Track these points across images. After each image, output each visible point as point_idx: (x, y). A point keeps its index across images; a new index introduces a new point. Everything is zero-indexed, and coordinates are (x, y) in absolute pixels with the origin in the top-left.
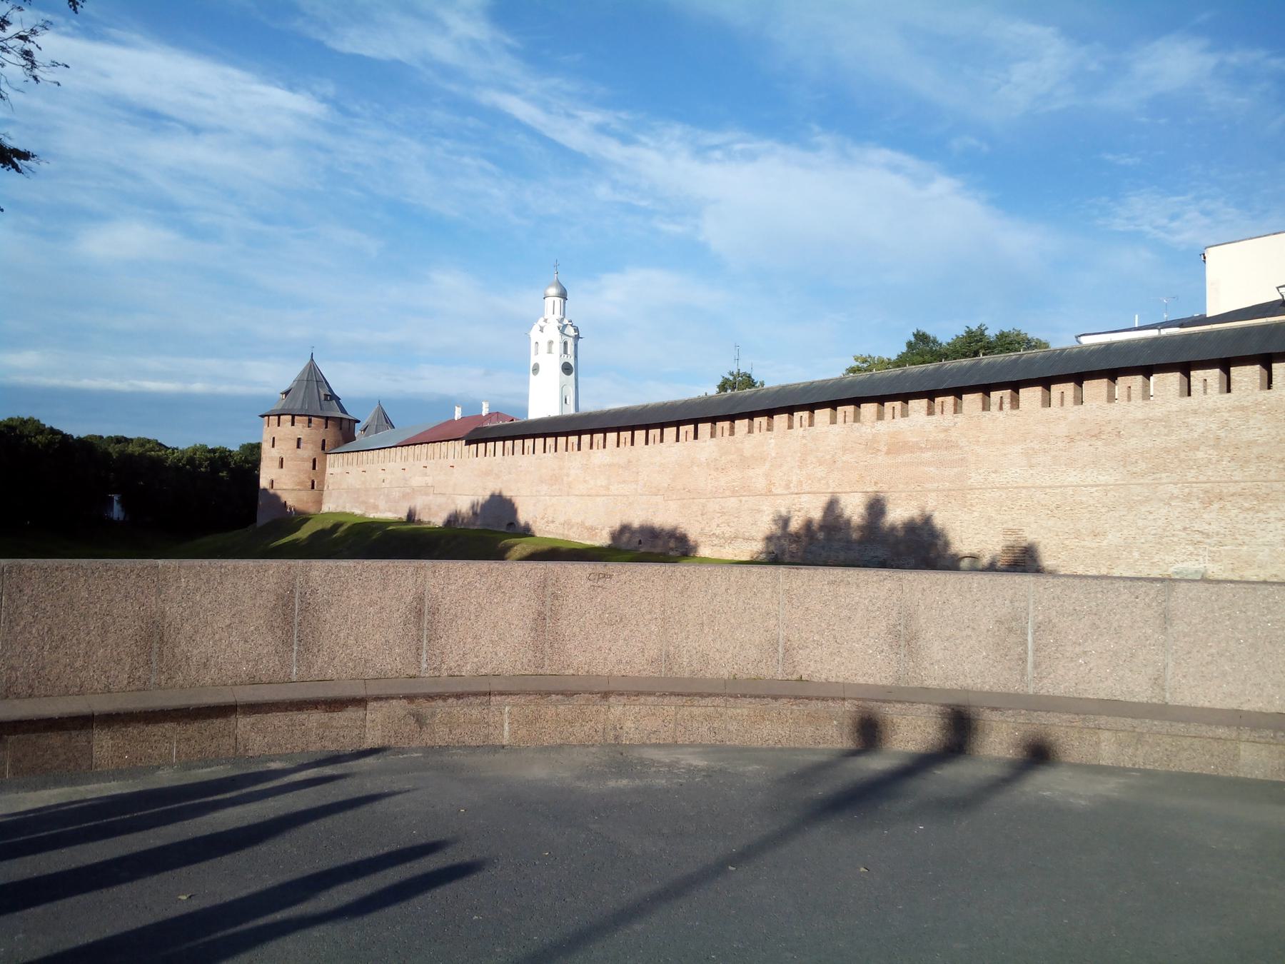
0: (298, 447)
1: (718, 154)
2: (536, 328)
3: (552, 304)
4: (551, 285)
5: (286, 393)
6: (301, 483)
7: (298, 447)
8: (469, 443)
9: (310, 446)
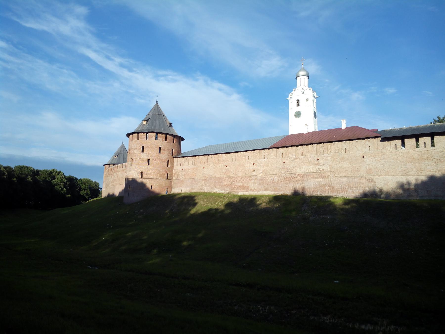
0: (160, 152)
1: (162, 78)
5: (147, 121)
6: (161, 175)
7: (160, 152)
8: (383, 140)
9: (166, 152)
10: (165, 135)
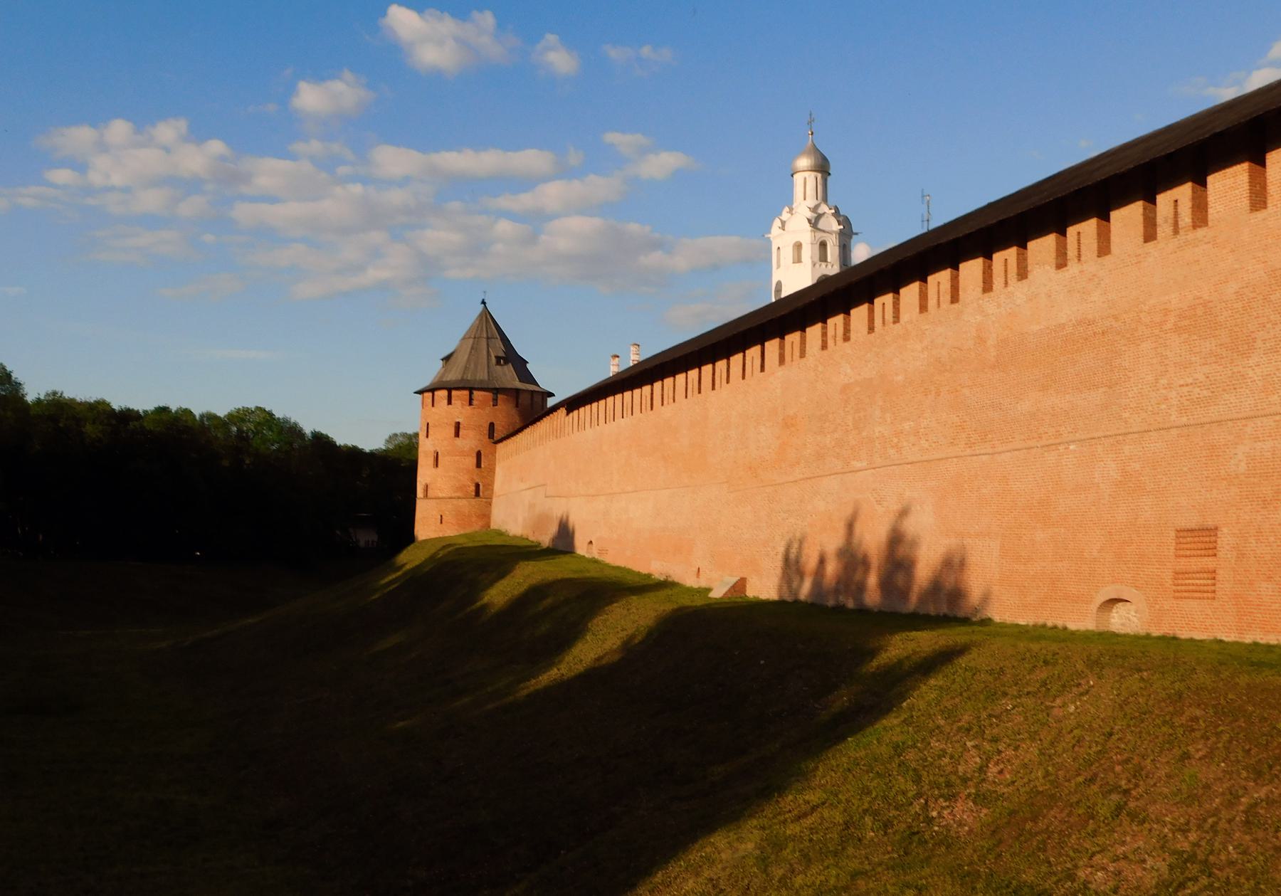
0: (457, 435)
2: (777, 223)
3: (805, 182)
4: (802, 153)
5: (447, 359)
7: (457, 435)
9: (471, 433)
10: (466, 393)
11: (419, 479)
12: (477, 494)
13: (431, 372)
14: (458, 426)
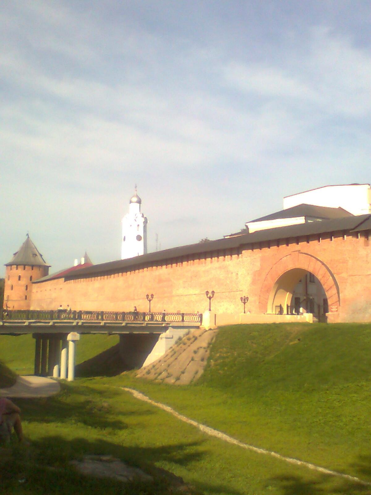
0: (19, 279)
5: (15, 254)
7: (19, 279)
9: (25, 279)
11: (5, 294)
12: (26, 299)
13: (10, 259)
14: (20, 277)
